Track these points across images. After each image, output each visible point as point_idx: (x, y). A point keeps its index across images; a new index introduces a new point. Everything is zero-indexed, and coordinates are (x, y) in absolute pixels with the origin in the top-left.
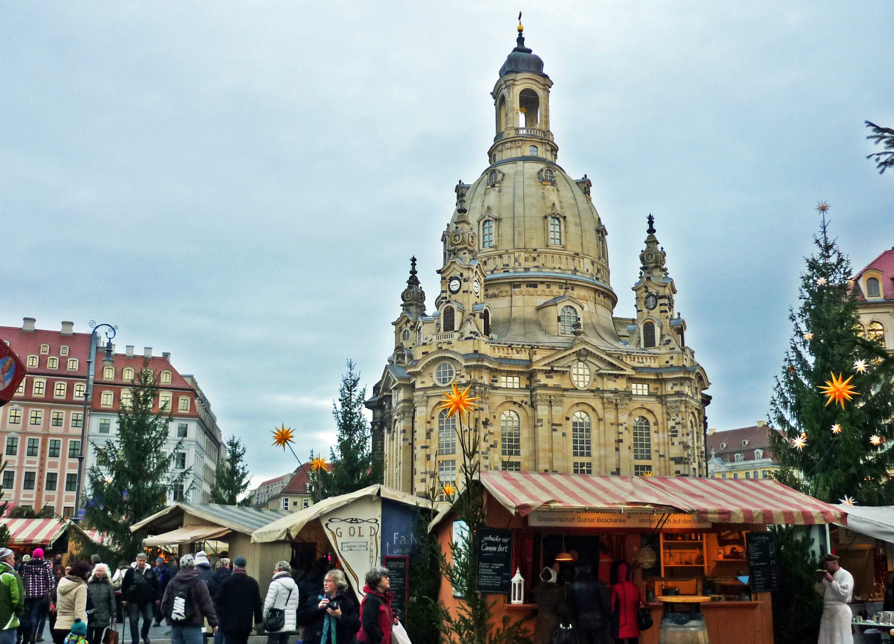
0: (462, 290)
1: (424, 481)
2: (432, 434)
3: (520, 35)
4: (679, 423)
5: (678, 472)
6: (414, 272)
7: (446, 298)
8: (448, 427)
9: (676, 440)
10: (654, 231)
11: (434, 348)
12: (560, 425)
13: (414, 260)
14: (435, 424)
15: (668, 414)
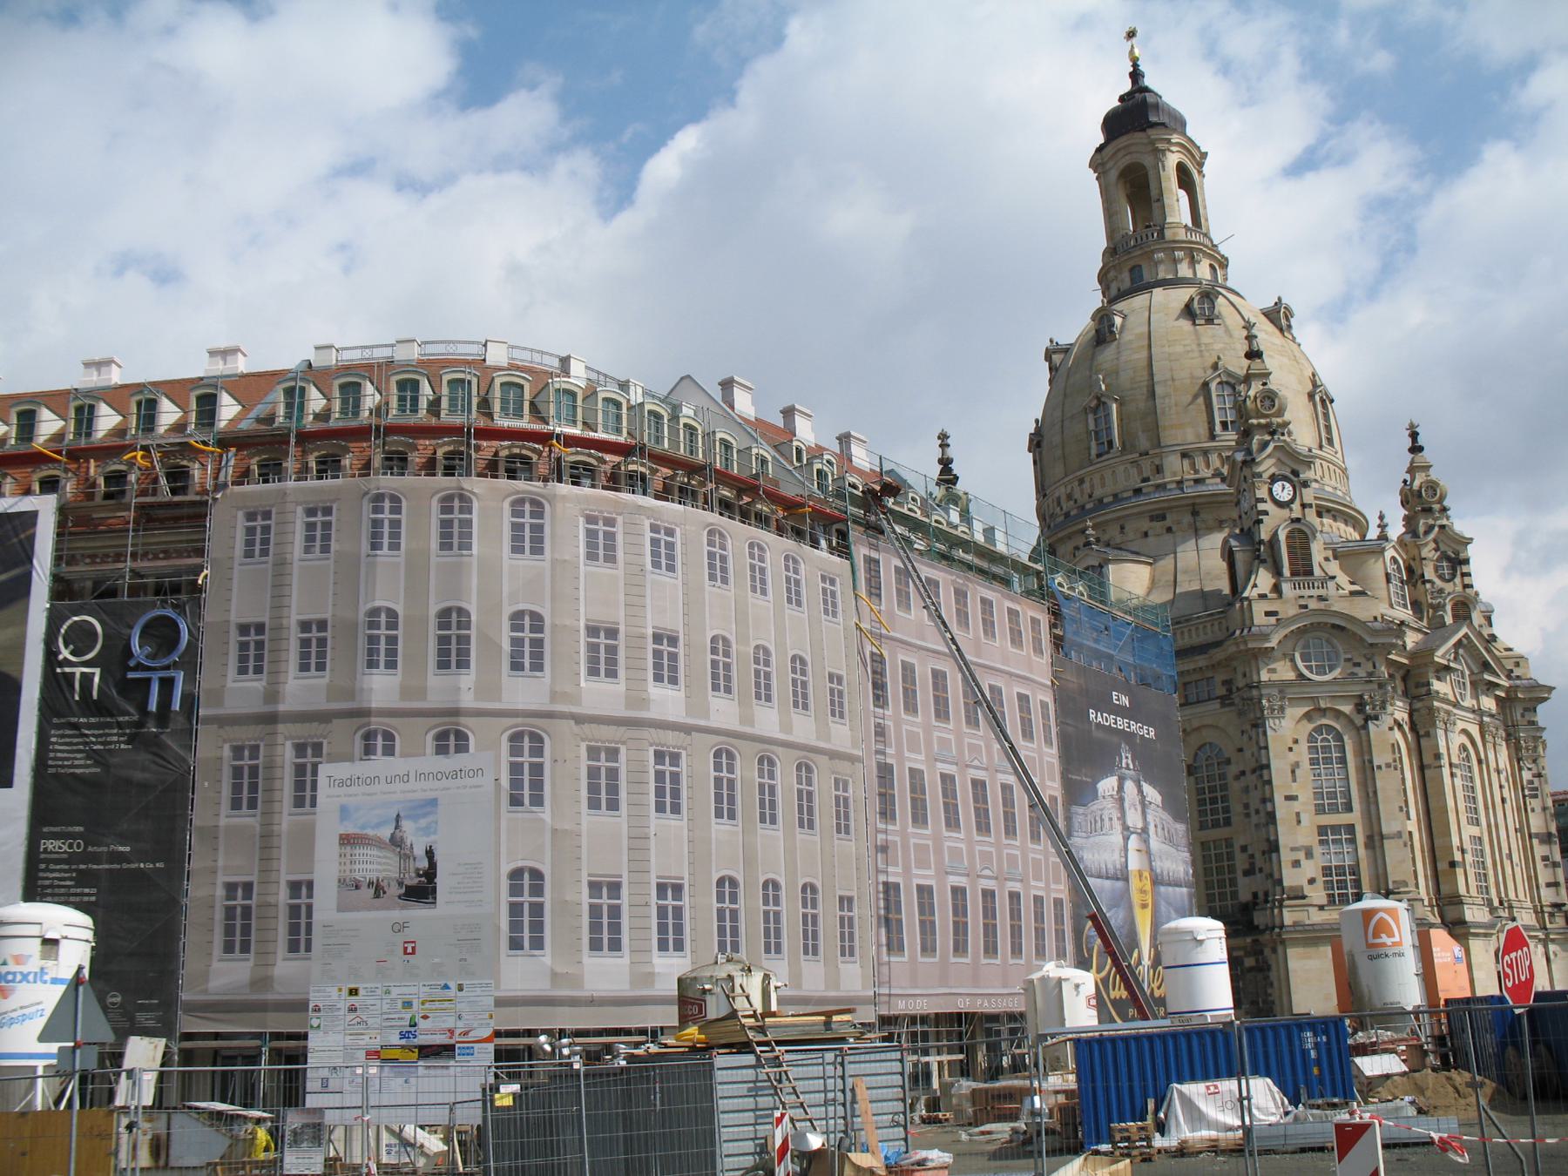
0: (1298, 502)
1: (1296, 864)
2: (1298, 772)
3: (1135, 65)
4: (1539, 775)
5: (1545, 858)
6: (946, 463)
7: (1266, 513)
8: (1328, 761)
9: (1535, 803)
10: (1421, 449)
11: (1288, 610)
12: (1457, 766)
13: (943, 437)
14: (1303, 753)
15: (1519, 761)
